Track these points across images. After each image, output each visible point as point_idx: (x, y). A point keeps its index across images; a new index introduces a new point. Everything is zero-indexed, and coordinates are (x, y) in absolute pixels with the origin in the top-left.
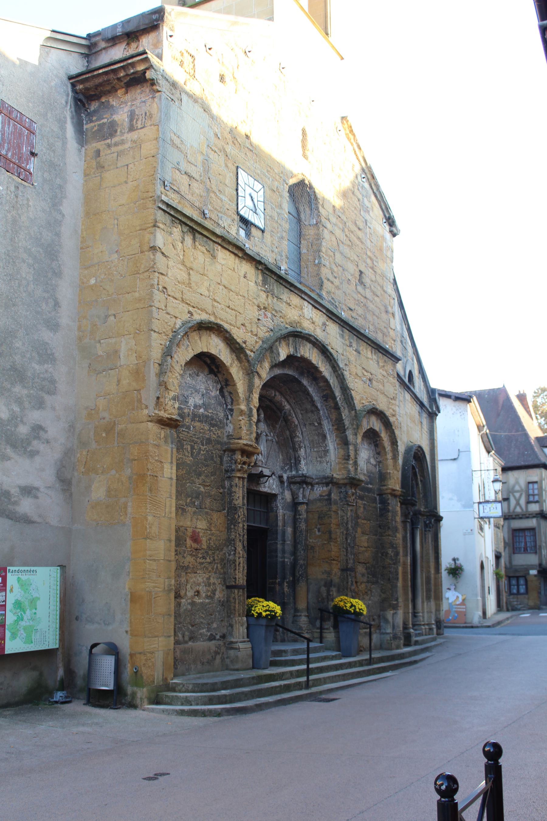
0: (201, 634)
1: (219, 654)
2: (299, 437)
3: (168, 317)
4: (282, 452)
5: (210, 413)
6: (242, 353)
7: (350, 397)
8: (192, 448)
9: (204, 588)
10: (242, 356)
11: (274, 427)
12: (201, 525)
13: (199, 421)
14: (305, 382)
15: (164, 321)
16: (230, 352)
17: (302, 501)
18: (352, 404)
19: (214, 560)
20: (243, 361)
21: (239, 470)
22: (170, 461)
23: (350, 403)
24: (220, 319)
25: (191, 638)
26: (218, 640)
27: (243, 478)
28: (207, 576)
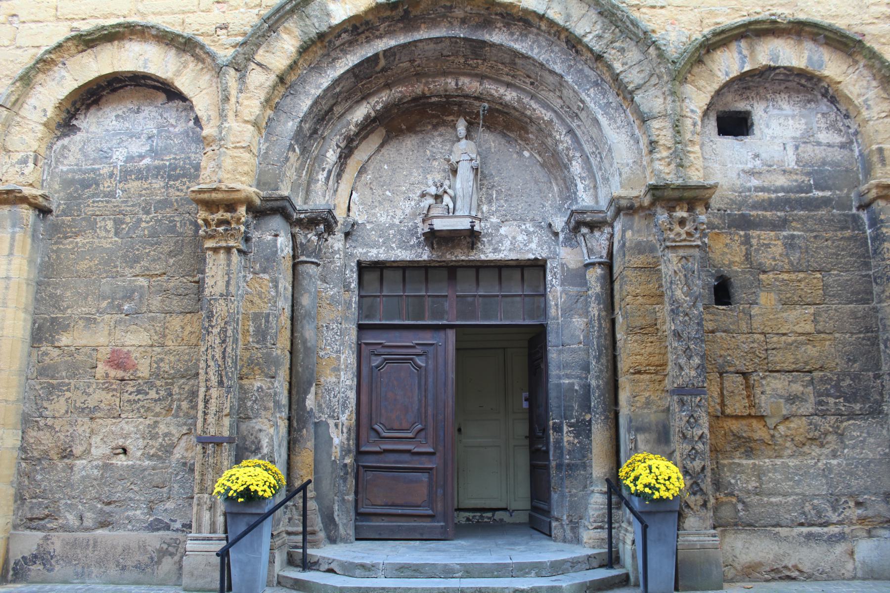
0: (128, 518)
1: (172, 555)
2: (562, 142)
3: (19, 52)
4: (556, 179)
5: (167, 160)
6: (196, 47)
7: (628, 23)
8: (118, 223)
9: (141, 443)
10: (197, 50)
11: (526, 140)
12: (135, 340)
13: (137, 179)
14: (497, 37)
15: (6, 60)
16: (178, 55)
17: (589, 261)
18: (641, 35)
19: (171, 395)
20: (203, 59)
21: (212, 237)
22: (6, 252)
23: (635, 34)
24: (154, 13)
25: (103, 525)
26: (177, 530)
27: (228, 250)
28: (151, 422)
